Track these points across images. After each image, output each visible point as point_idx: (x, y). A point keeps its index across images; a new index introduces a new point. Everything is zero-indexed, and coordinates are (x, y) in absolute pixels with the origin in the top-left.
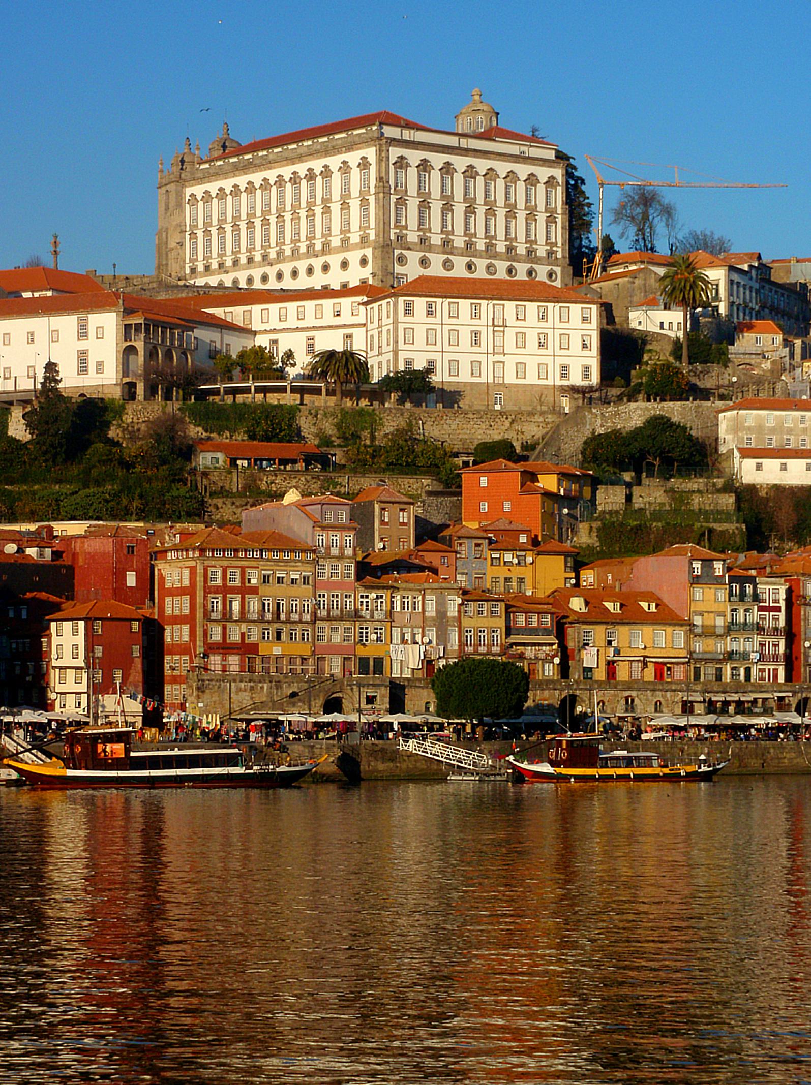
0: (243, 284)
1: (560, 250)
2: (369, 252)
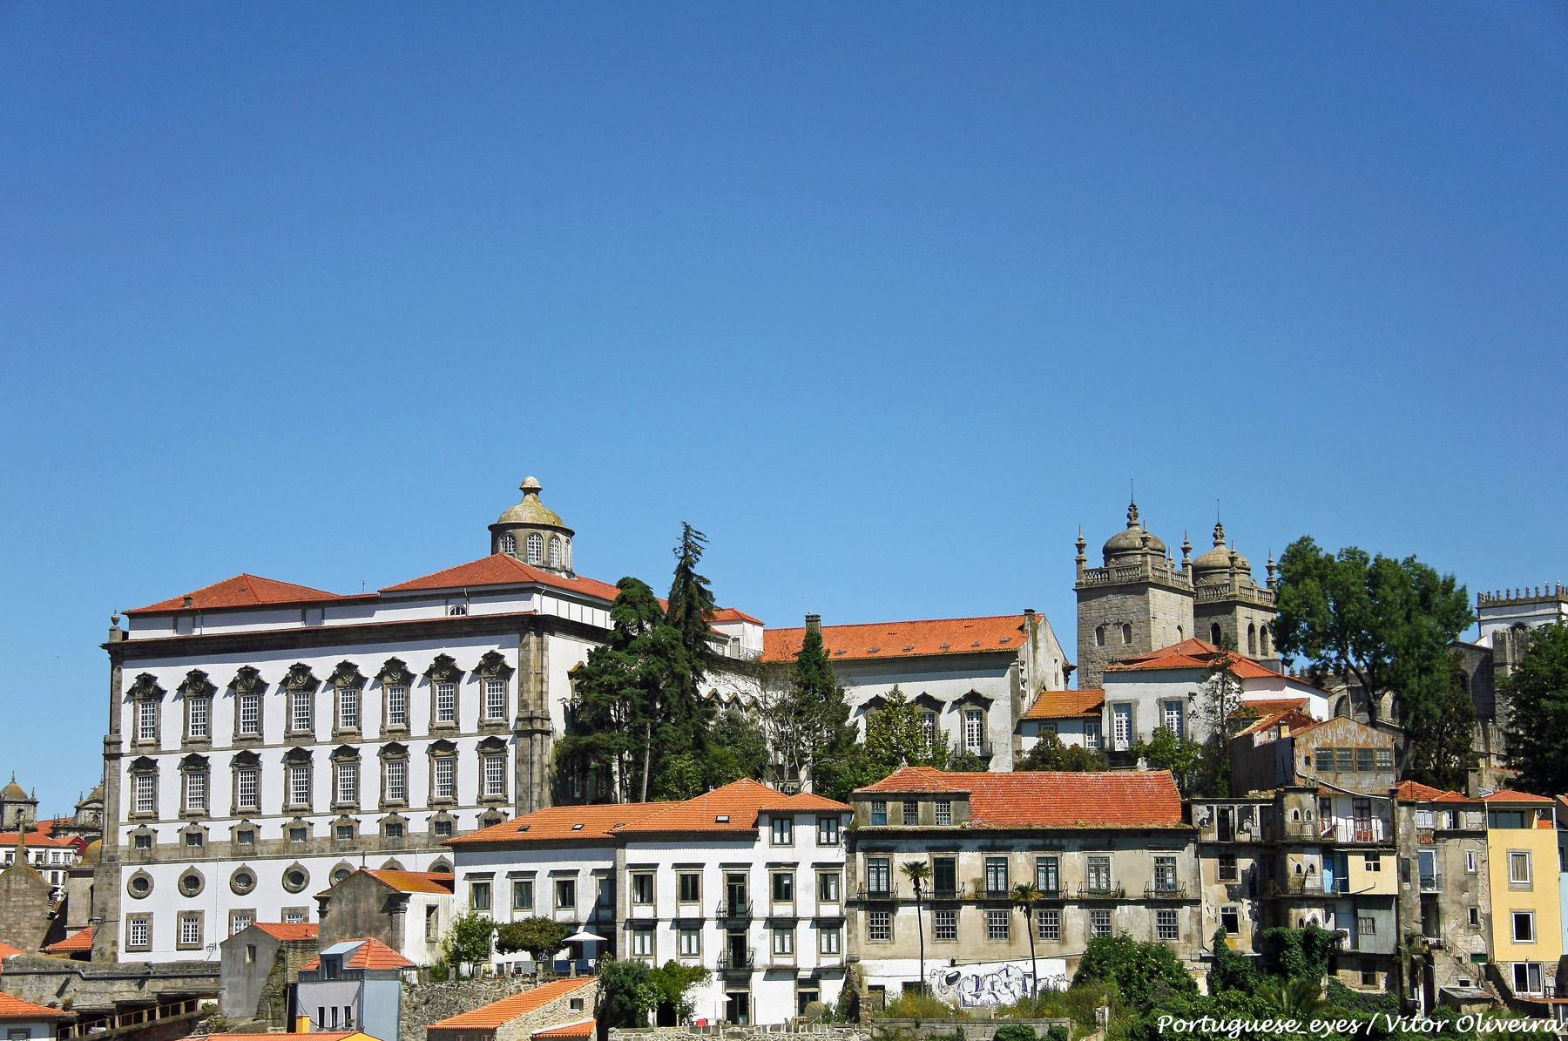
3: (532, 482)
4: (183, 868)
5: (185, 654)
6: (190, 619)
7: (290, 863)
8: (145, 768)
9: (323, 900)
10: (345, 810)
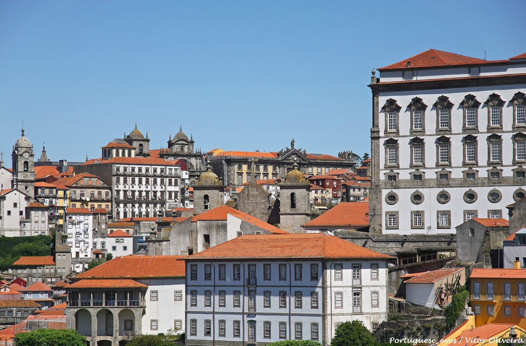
5: (411, 90)
6: (411, 72)
7: (467, 189)
8: (392, 144)
9: (511, 209)
10: (495, 165)
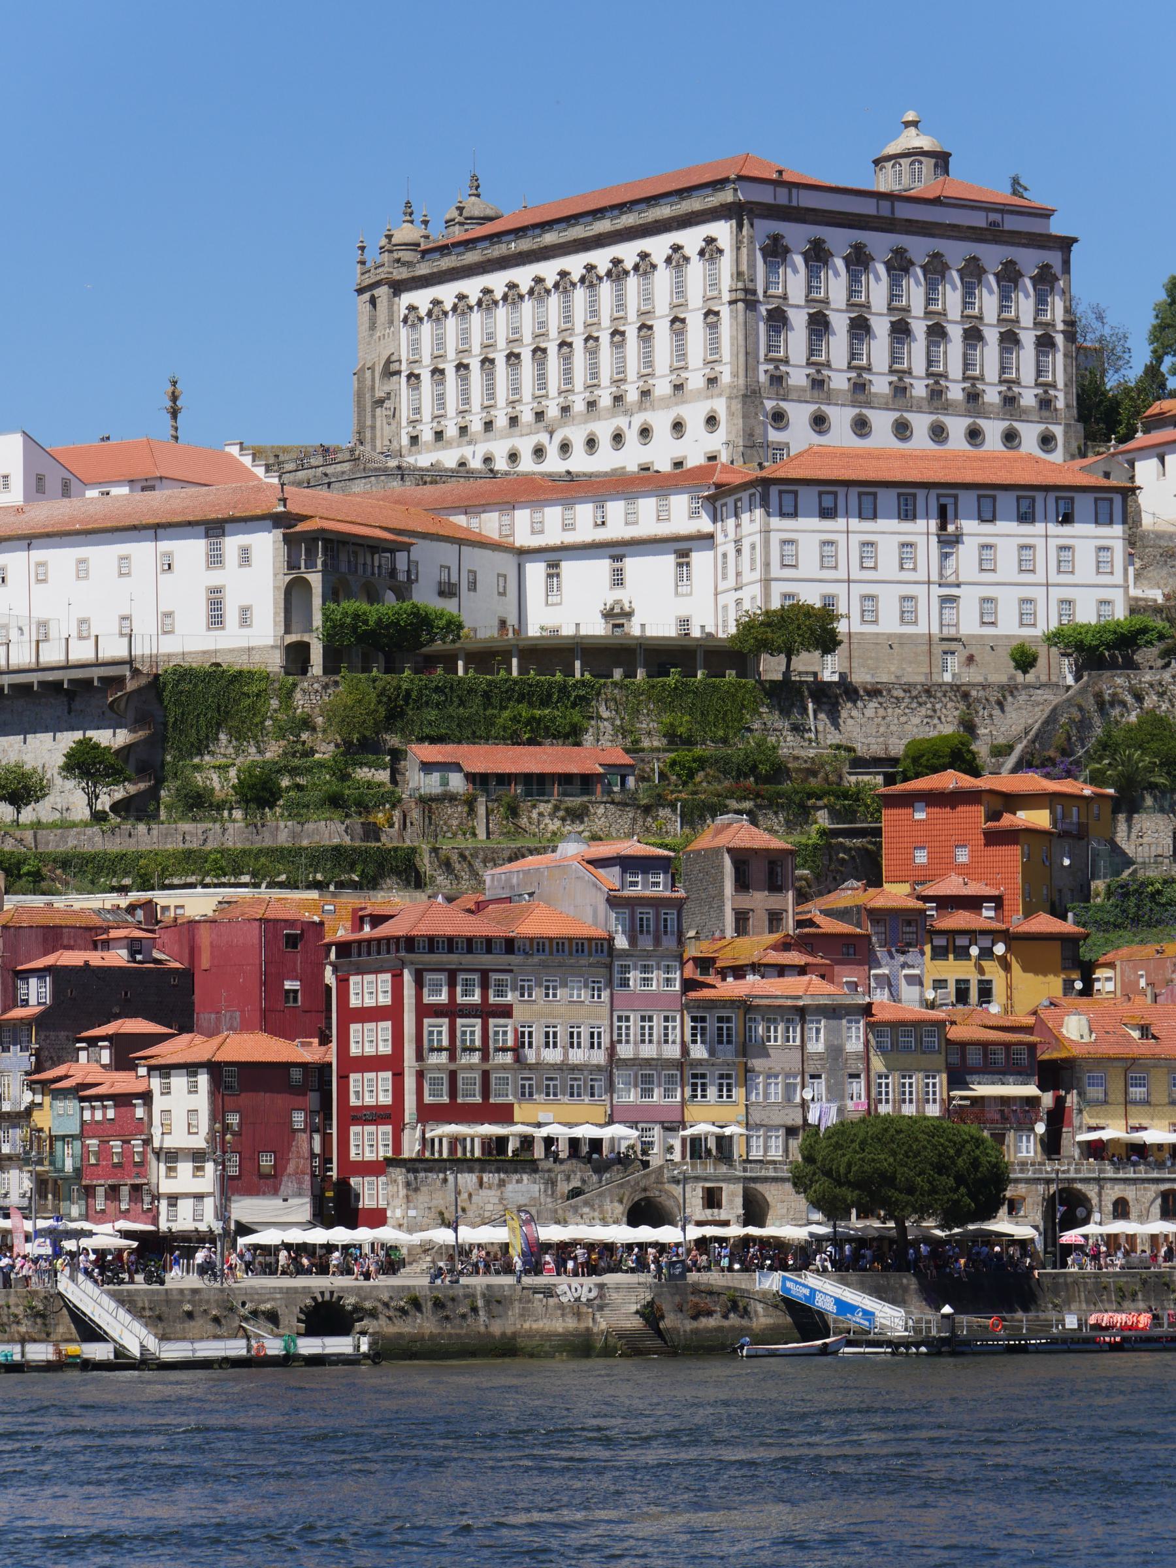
0: (501, 464)
1: (1061, 395)
2: (720, 406)
3: (910, 116)
4: (812, 408)
10: (936, 378)
